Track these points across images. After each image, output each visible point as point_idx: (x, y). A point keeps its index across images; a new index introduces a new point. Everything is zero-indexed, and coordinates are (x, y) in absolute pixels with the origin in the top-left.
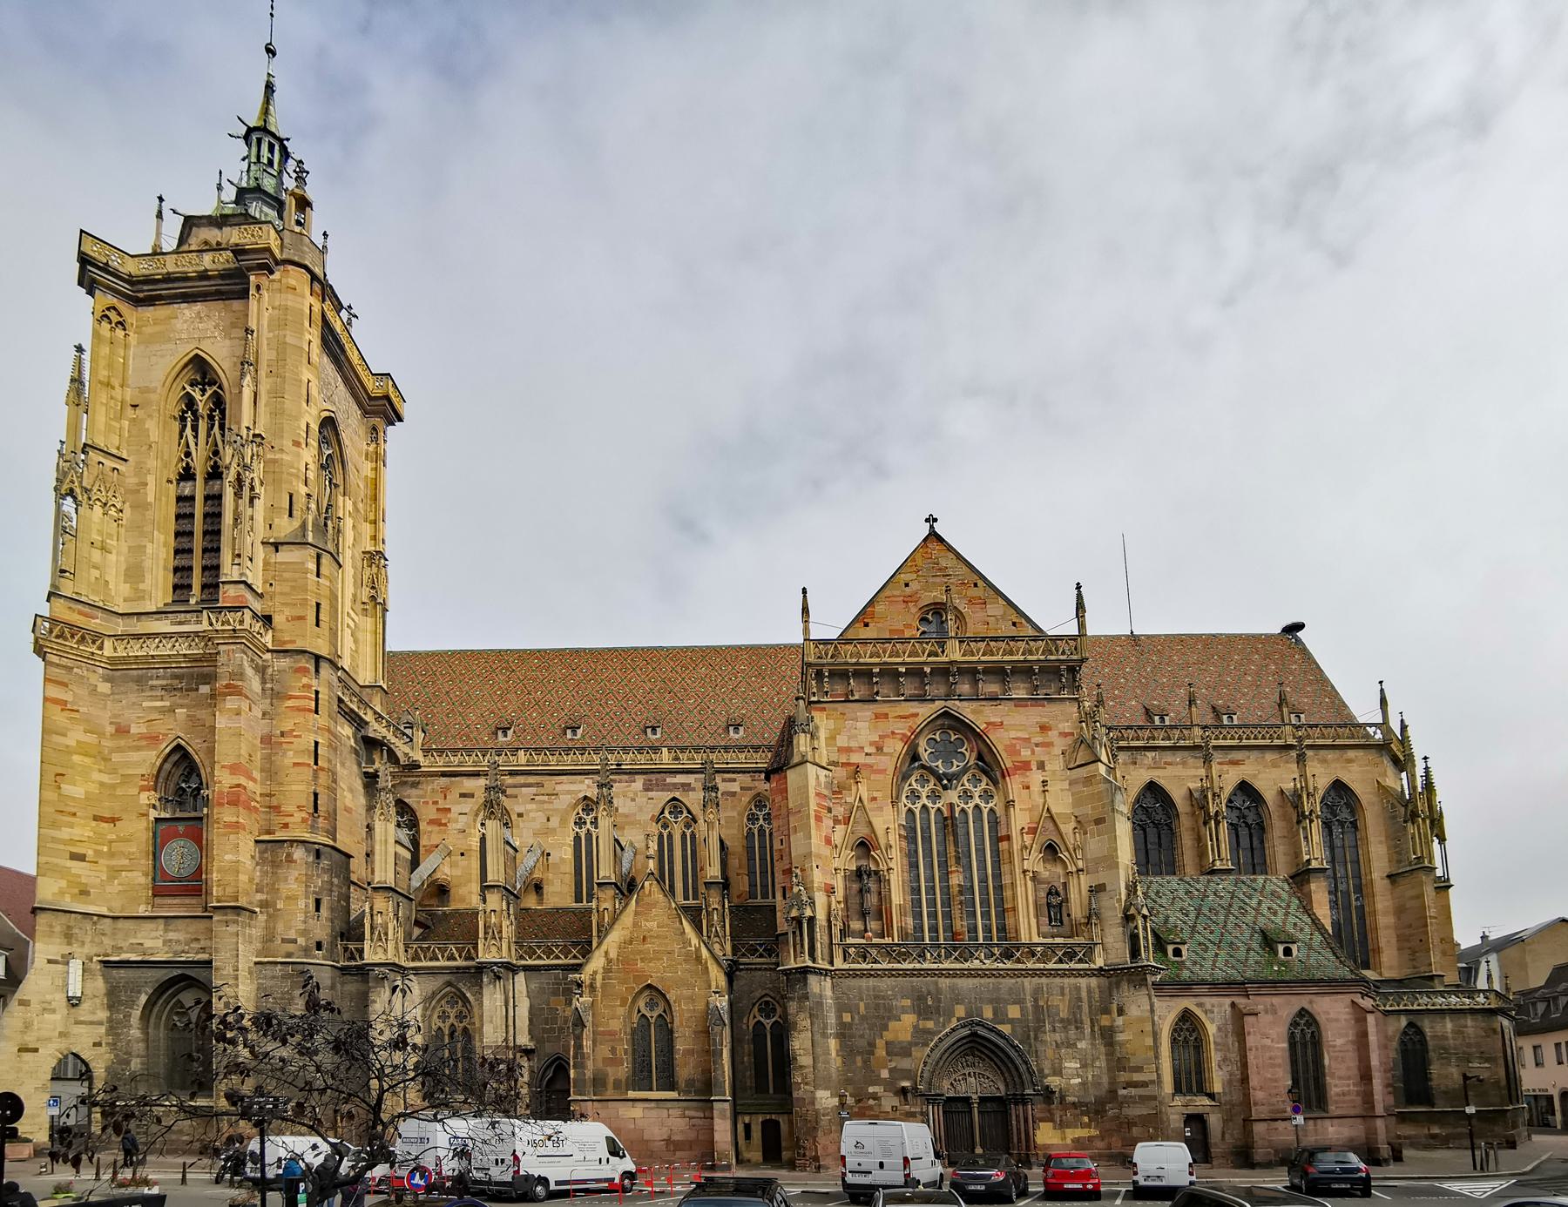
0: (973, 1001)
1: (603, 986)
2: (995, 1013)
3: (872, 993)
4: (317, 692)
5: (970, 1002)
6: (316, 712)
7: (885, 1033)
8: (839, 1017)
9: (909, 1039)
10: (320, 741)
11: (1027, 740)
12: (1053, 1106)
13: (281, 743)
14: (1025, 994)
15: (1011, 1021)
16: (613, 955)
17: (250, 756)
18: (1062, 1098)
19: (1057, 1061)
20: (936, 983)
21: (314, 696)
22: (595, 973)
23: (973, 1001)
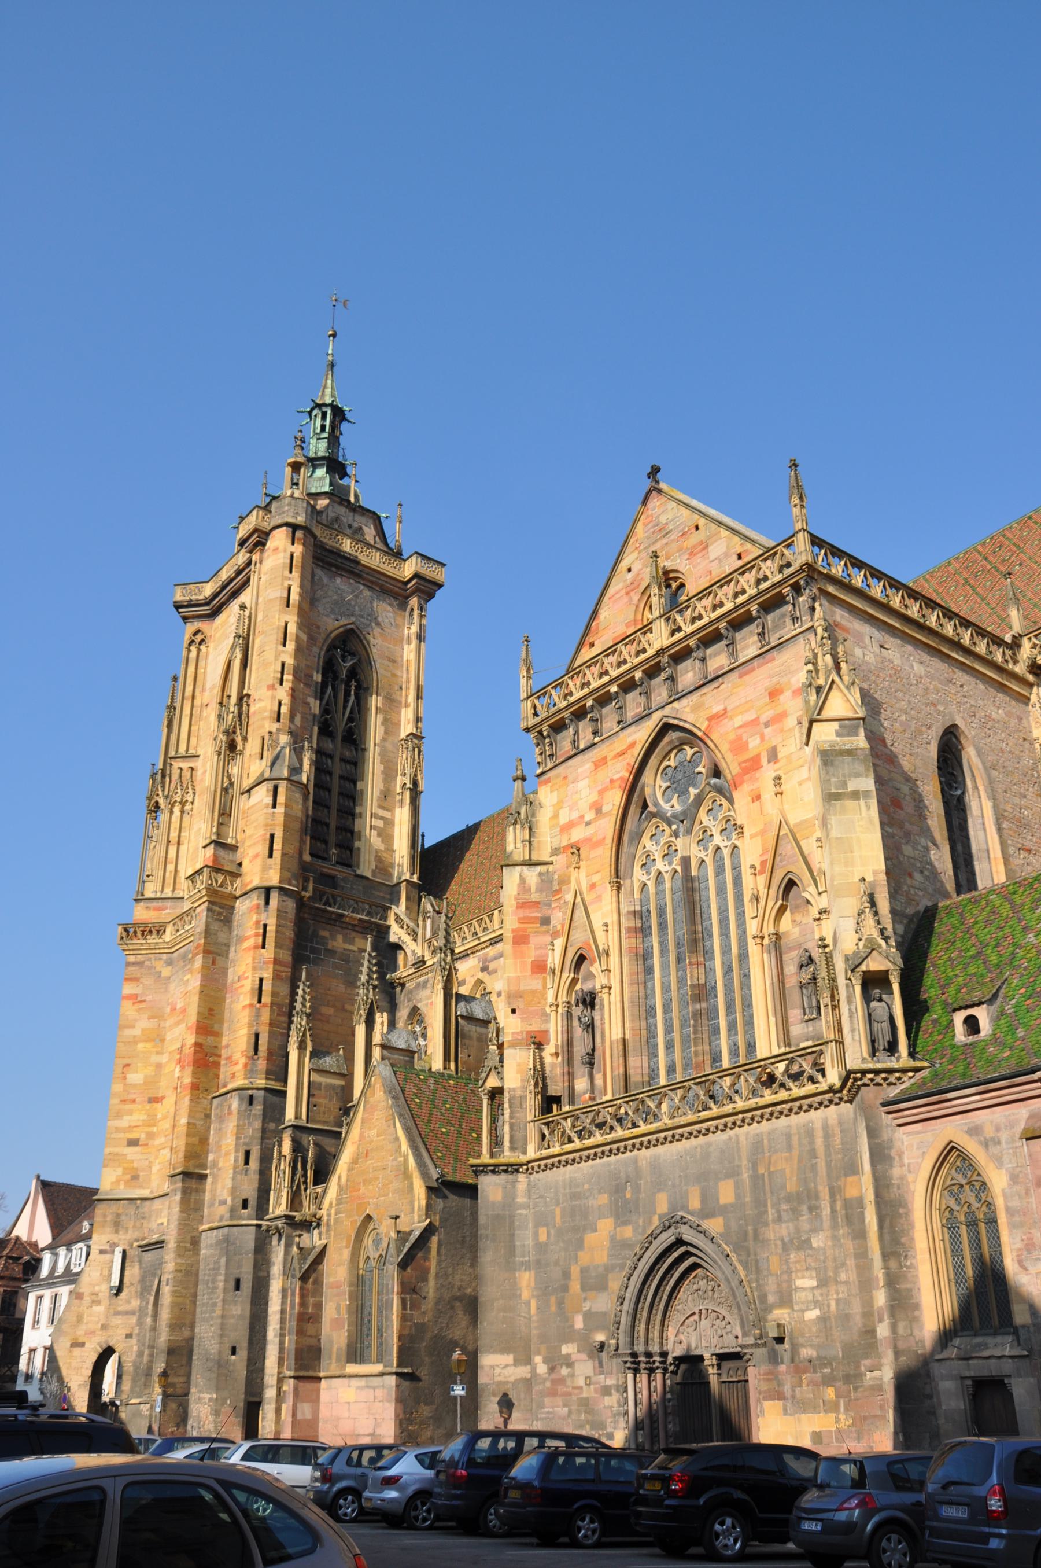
0: (677, 1182)
1: (335, 1219)
2: (704, 1199)
3: (567, 1191)
4: (265, 926)
5: (674, 1186)
6: (263, 947)
7: (580, 1254)
8: (536, 1234)
9: (605, 1259)
10: (265, 975)
11: (755, 722)
12: (783, 1368)
14: (740, 1157)
15: (723, 1211)
16: (343, 1180)
17: (211, 1010)
18: (795, 1349)
19: (785, 1277)
20: (635, 1160)
21: (261, 931)
22: (331, 1204)
23: (677, 1182)
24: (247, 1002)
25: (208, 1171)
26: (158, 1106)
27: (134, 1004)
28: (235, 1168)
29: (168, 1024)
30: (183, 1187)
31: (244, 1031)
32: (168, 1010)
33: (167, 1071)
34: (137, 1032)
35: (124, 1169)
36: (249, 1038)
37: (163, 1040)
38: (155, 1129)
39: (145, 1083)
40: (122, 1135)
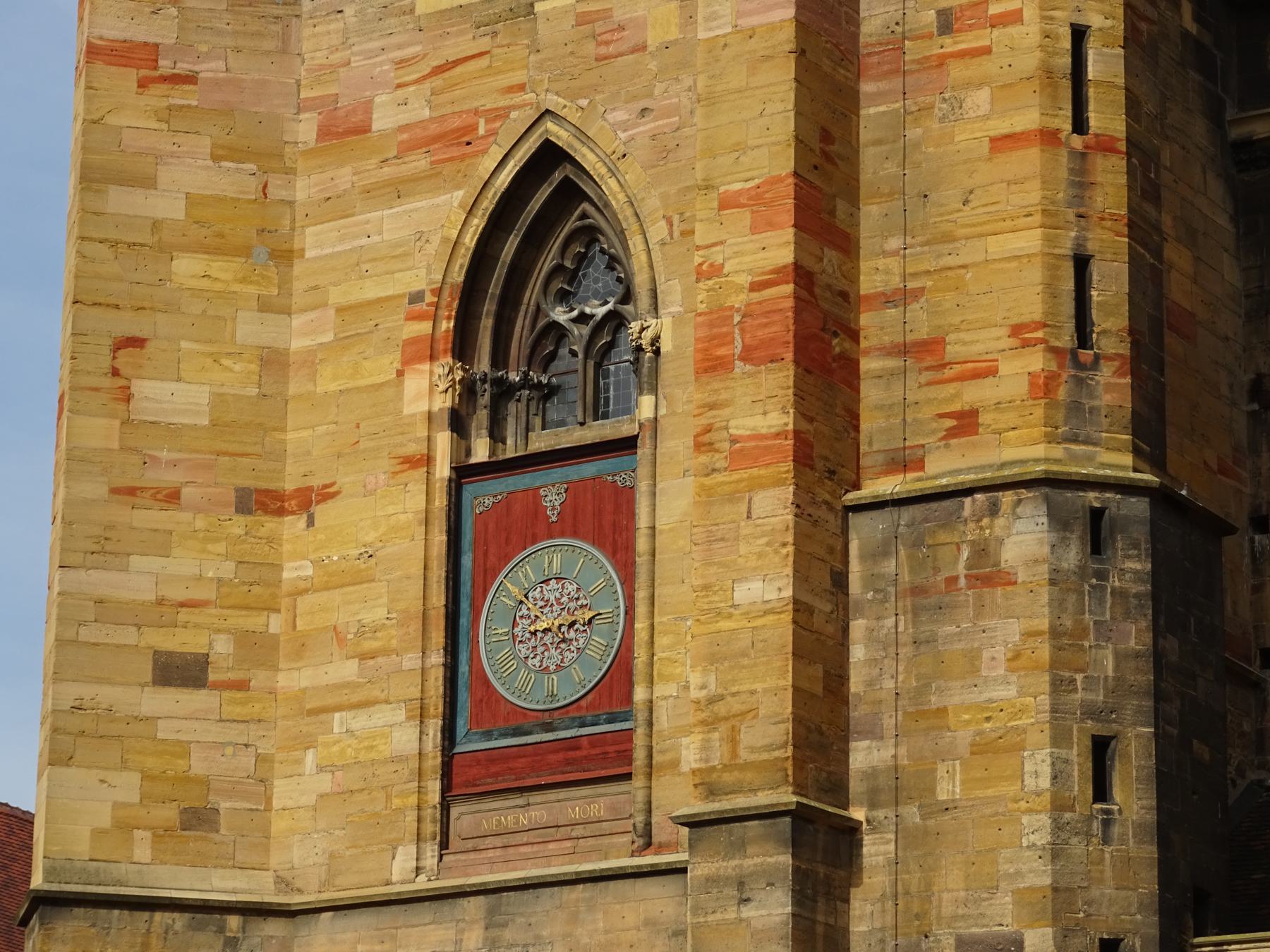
10: (1095, 20)
13: (942, 62)
17: (826, 137)
24: (1028, 119)
25: (858, 814)
26: (293, 525)
27: (143, 84)
28: (1059, 806)
29: (304, 189)
30: (796, 870)
31: (1030, 240)
32: (306, 130)
33: (327, 383)
34: (169, 207)
35: (146, 777)
36: (1052, 269)
37: (285, 256)
38: (276, 624)
39: (214, 424)
40: (129, 636)
